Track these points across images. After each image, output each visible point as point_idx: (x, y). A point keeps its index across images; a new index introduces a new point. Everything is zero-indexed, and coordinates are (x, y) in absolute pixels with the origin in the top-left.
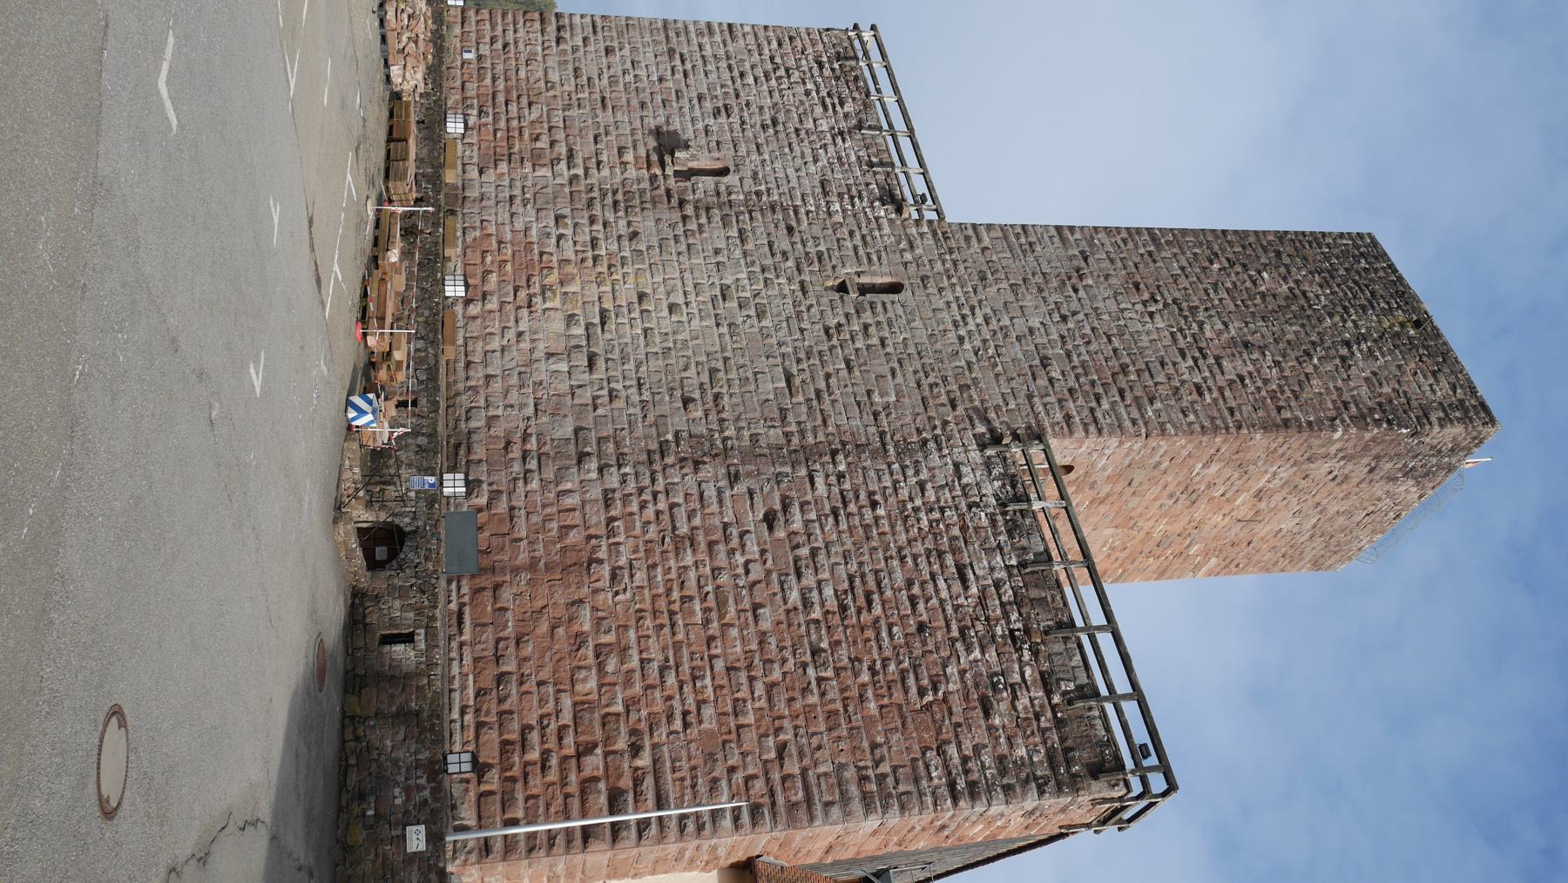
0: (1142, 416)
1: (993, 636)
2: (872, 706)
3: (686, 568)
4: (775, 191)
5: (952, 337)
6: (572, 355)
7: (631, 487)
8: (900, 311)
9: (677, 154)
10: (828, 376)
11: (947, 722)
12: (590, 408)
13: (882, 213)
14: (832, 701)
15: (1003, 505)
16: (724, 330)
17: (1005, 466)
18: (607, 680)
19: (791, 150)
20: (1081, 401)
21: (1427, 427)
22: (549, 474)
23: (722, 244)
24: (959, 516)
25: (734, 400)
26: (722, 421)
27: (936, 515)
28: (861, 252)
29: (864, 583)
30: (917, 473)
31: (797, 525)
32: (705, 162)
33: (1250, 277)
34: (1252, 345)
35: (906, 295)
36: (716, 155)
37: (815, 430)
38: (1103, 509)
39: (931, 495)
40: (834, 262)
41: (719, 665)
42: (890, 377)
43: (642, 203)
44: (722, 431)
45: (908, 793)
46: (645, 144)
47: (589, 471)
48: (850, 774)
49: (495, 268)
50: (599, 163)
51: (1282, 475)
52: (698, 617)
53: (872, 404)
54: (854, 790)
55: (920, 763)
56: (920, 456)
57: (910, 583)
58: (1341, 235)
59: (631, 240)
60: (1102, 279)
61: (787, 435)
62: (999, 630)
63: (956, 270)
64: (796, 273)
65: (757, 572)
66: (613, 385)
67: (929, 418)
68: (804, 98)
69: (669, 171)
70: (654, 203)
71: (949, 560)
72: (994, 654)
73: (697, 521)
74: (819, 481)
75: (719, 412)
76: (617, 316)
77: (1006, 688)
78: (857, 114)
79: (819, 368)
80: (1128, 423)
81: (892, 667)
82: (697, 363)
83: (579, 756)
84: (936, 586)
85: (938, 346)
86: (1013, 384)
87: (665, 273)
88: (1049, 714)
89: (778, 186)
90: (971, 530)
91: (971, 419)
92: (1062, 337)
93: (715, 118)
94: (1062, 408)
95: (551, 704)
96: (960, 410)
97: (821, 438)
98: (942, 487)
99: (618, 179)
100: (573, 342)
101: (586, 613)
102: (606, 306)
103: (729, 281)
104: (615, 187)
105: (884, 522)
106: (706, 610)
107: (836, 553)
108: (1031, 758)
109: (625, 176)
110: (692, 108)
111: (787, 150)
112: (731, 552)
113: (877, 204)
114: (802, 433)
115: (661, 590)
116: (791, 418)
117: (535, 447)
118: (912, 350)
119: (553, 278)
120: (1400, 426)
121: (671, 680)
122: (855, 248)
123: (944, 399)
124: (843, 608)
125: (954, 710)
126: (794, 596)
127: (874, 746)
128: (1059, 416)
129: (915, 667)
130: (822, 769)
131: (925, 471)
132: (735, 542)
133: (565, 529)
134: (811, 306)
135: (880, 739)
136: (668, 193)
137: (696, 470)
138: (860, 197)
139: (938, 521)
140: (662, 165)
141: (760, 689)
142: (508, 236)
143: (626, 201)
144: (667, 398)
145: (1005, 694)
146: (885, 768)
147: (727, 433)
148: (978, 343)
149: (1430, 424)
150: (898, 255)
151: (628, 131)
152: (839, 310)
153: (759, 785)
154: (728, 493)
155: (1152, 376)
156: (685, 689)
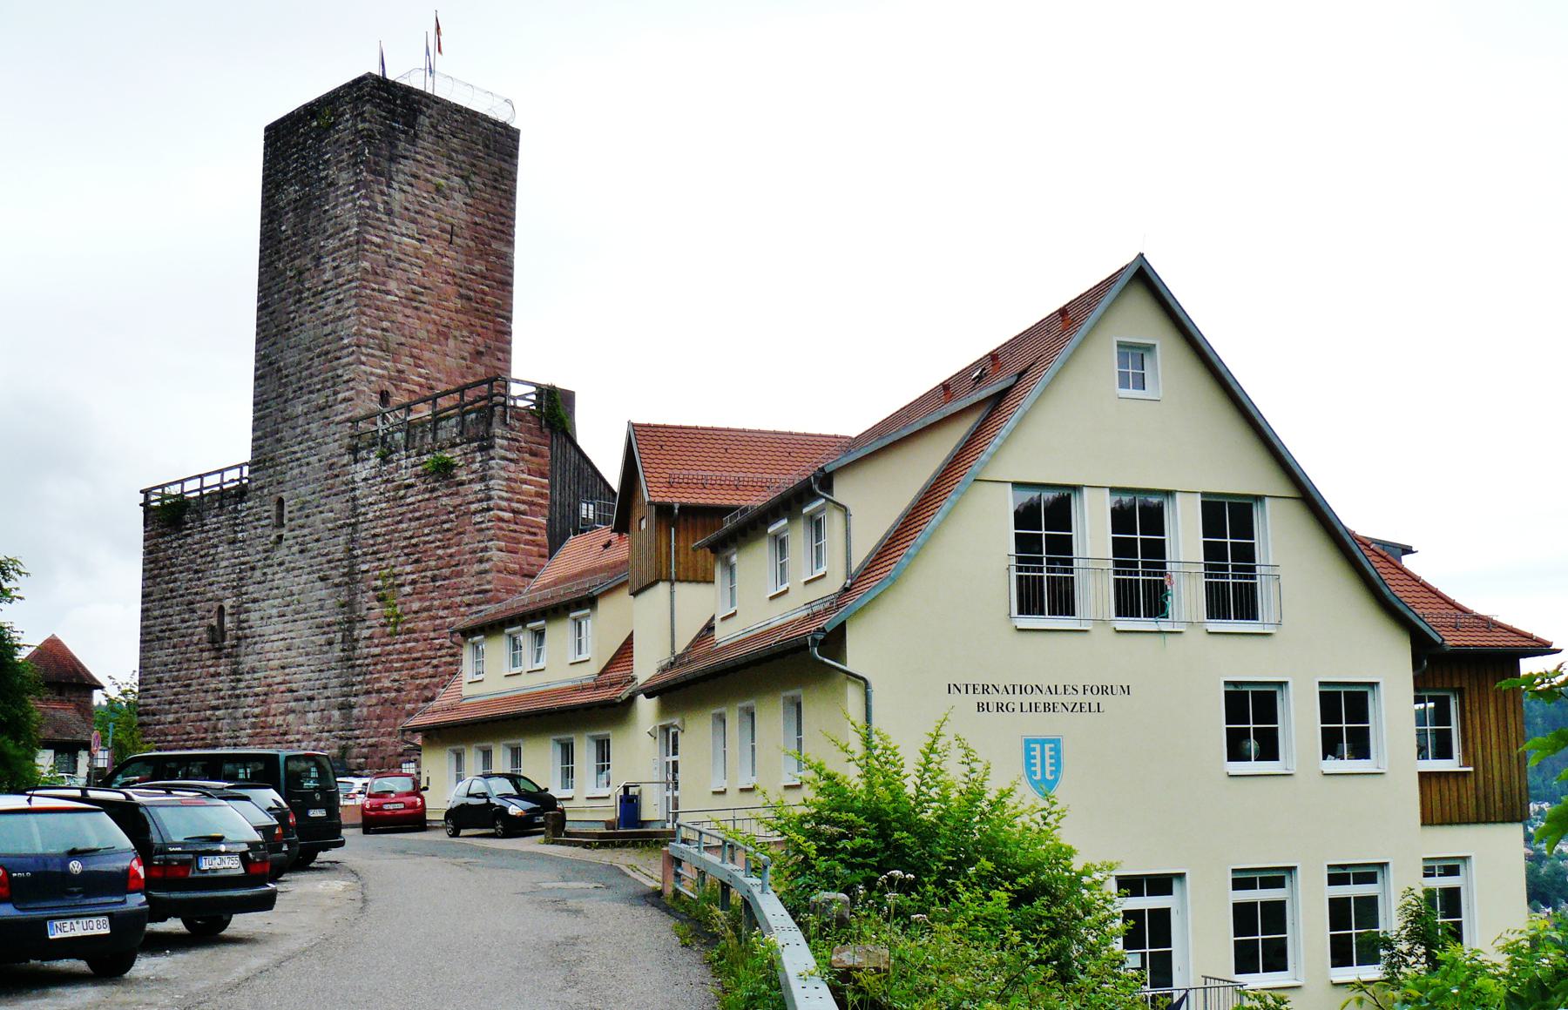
0: (348, 347)
35: (285, 495)
70: (237, 656)
74: (364, 567)
88: (464, 446)
103: (274, 612)
121: (435, 662)
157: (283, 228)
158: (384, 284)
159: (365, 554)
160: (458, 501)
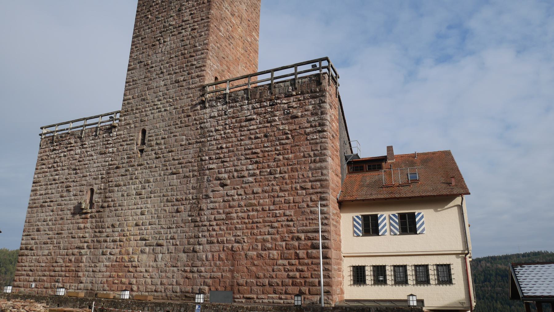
0: (200, 50)
1: (271, 112)
2: (291, 156)
3: (237, 217)
4: (102, 172)
5: (164, 114)
6: (156, 252)
7: (207, 234)
8: (152, 131)
9: (83, 207)
10: (174, 159)
11: (298, 131)
12: (177, 247)
13: (115, 133)
14: (288, 169)
15: (226, 103)
16: (152, 195)
17: (213, 100)
18: (274, 247)
19: (86, 164)
20: (193, 71)
22: (199, 263)
23: (120, 193)
24: (228, 119)
26: (186, 199)
27: (227, 126)
28: (129, 142)
29: (248, 154)
30: (212, 132)
31: (226, 176)
32: (88, 197)
35: (147, 128)
36: (85, 193)
37: (193, 166)
38: (232, 69)
39: (220, 128)
40: (132, 153)
41: (272, 207)
42: (176, 137)
43: (101, 222)
44: (190, 199)
45: (321, 147)
46: (78, 219)
47: (200, 249)
48: (312, 166)
49: (120, 279)
50: (83, 237)
52: (255, 213)
53: (185, 145)
54: (318, 165)
55: (311, 141)
56: (206, 130)
57: (250, 138)
59: (114, 227)
60: (149, 57)
61: (193, 176)
62: (269, 110)
63: (140, 109)
64: (134, 167)
65: (241, 191)
66: (169, 238)
67: (193, 125)
68: (67, 157)
69: (89, 211)
70: (101, 217)
72: (277, 112)
73: (221, 211)
75: (183, 200)
76: (143, 235)
78: (76, 138)
79: (170, 162)
80: (202, 56)
81: (278, 148)
82: (164, 206)
83: (299, 259)
84: (252, 129)
85: (167, 119)
86: (184, 94)
87: (129, 216)
88: (299, 96)
89: (100, 171)
91: (195, 110)
92: (169, 74)
93: (70, 192)
94: (194, 78)
95: (281, 267)
96: (191, 114)
97: (196, 164)
98: (218, 123)
99: (91, 230)
100: (151, 251)
101: (250, 253)
103: (134, 192)
104: (93, 232)
105: (229, 145)
106: (253, 210)
107: (237, 163)
108: (313, 104)
109: (89, 227)
110: (65, 200)
111: (86, 166)
112: (233, 200)
113: (111, 135)
114: (193, 171)
115: (244, 226)
116: (187, 174)
117: (189, 268)
118: (167, 128)
119: (126, 258)
122: (127, 144)
123: (186, 119)
124: (257, 162)
125: (294, 128)
126: (251, 179)
127: (304, 157)
128: (197, 79)
129: (279, 140)
130: (310, 175)
131: (211, 129)
132: (230, 198)
133: (220, 259)
134: (147, 163)
135: (302, 154)
136: (97, 212)
137: (203, 210)
138: (108, 140)
139: (230, 126)
141: (281, 194)
142: (108, 273)
143: (99, 228)
144: (176, 218)
145: (291, 110)
146: (312, 154)
147: (191, 198)
148: (168, 105)
150: (132, 129)
151: (72, 225)
152: (150, 153)
153: (314, 197)
154: (212, 199)
156: (279, 220)
160: (293, 127)
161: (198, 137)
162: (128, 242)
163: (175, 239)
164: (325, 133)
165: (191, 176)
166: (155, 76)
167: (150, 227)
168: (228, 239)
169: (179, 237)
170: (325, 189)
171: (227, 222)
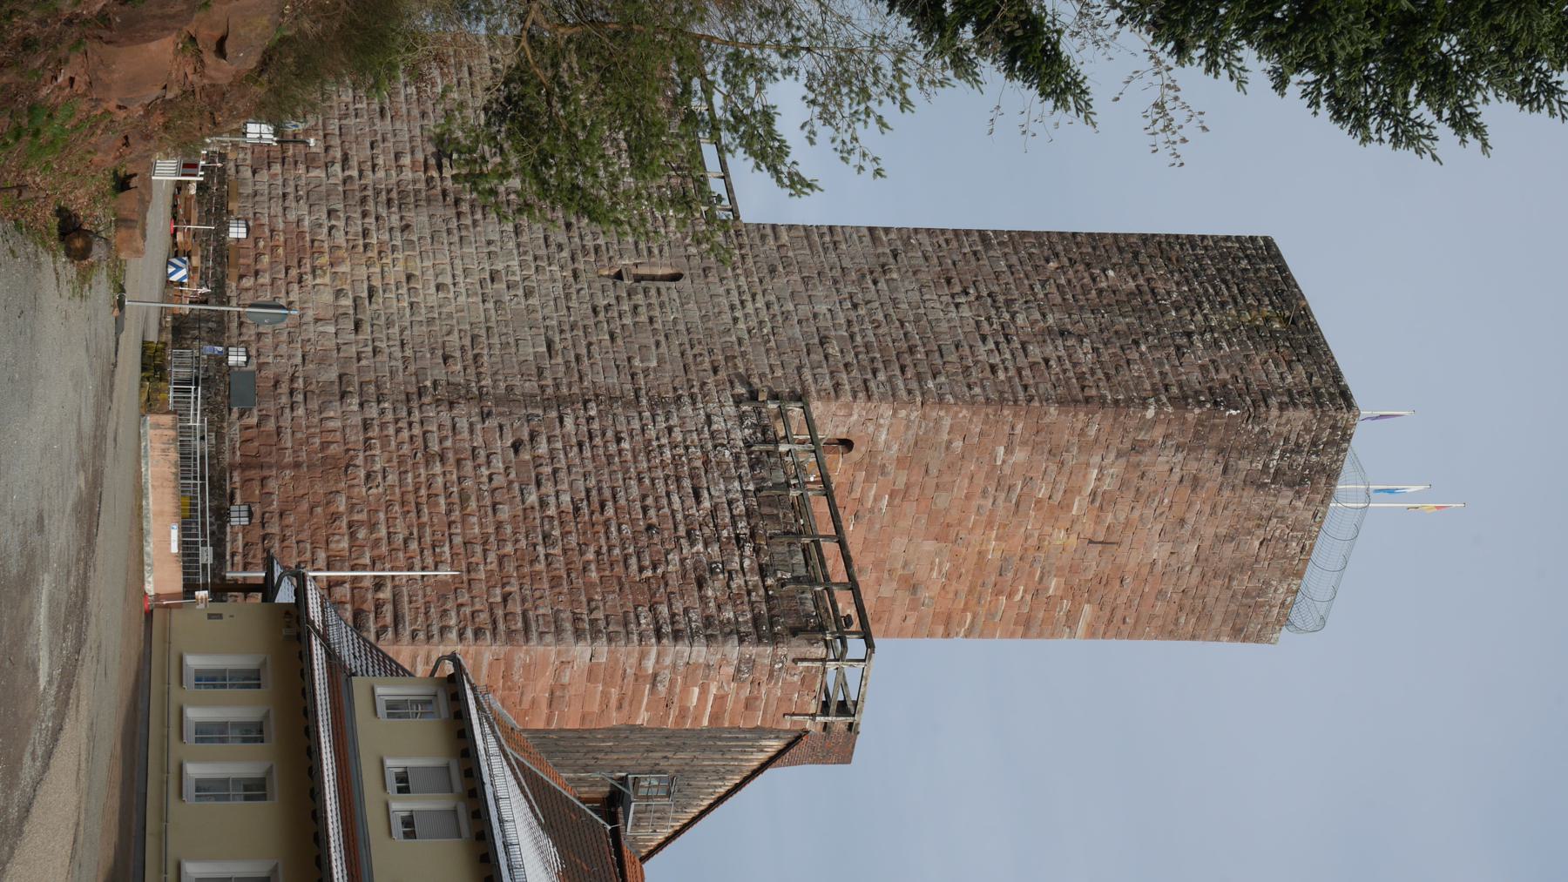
0: (921, 387)
2: (594, 575)
3: (434, 475)
5: (727, 318)
6: (340, 320)
8: (675, 295)
10: (590, 344)
11: (662, 590)
12: (355, 360)
15: (748, 445)
16: (490, 305)
18: (358, 543)
21: (1263, 409)
22: (314, 405)
23: (496, 237)
24: (703, 453)
25: (493, 359)
26: (479, 374)
27: (681, 451)
30: (667, 420)
33: (1091, 275)
34: (1070, 333)
35: (685, 283)
37: (570, 386)
39: (678, 436)
40: (611, 254)
41: (458, 540)
42: (654, 348)
46: (424, 150)
47: (350, 404)
48: (567, 615)
49: (268, 251)
50: (374, 166)
51: (1111, 471)
52: (443, 508)
54: (568, 626)
55: (632, 615)
56: (673, 408)
57: (644, 497)
58: (1227, 238)
59: (402, 231)
60: (910, 274)
61: (542, 388)
62: (725, 533)
63: (743, 263)
64: (570, 262)
65: (499, 480)
67: (688, 380)
69: (447, 173)
70: (429, 200)
71: (687, 483)
72: (716, 547)
73: (448, 443)
74: (569, 422)
76: (384, 291)
77: (723, 572)
80: (903, 393)
81: (617, 551)
82: (460, 331)
85: (710, 324)
86: (785, 357)
87: (435, 258)
88: (762, 592)
90: (713, 463)
91: (732, 383)
92: (849, 322)
94: (832, 377)
95: (308, 555)
96: (722, 374)
97: (575, 389)
99: (394, 180)
100: (341, 311)
102: (374, 283)
103: (500, 266)
108: (736, 619)
109: (401, 177)
114: (557, 386)
115: (410, 488)
116: (547, 373)
117: (302, 386)
118: (682, 327)
119: (325, 260)
120: (1228, 407)
121: (414, 546)
123: (707, 365)
124: (577, 509)
125: (670, 582)
126: (533, 498)
130: (541, 611)
131: (675, 418)
132: (482, 459)
136: (444, 193)
139: (680, 456)
140: (440, 167)
141: (492, 557)
142: (281, 226)
143: (400, 199)
144: (428, 355)
145: (721, 576)
146: (599, 615)
147: (483, 383)
149: (1267, 406)
150: (682, 249)
151: (407, 138)
154: (479, 426)
155: (942, 356)
156: (426, 552)
157: (1111, 273)
158: (1024, 443)
159: (589, 419)
160: (674, 583)
161: (653, 392)
162: (363, 261)
163: (374, 355)
164: (653, 640)
165: (543, 383)
166: (845, 291)
167: (406, 304)
168: (377, 459)
169: (378, 365)
170: (504, 637)
171: (419, 455)
